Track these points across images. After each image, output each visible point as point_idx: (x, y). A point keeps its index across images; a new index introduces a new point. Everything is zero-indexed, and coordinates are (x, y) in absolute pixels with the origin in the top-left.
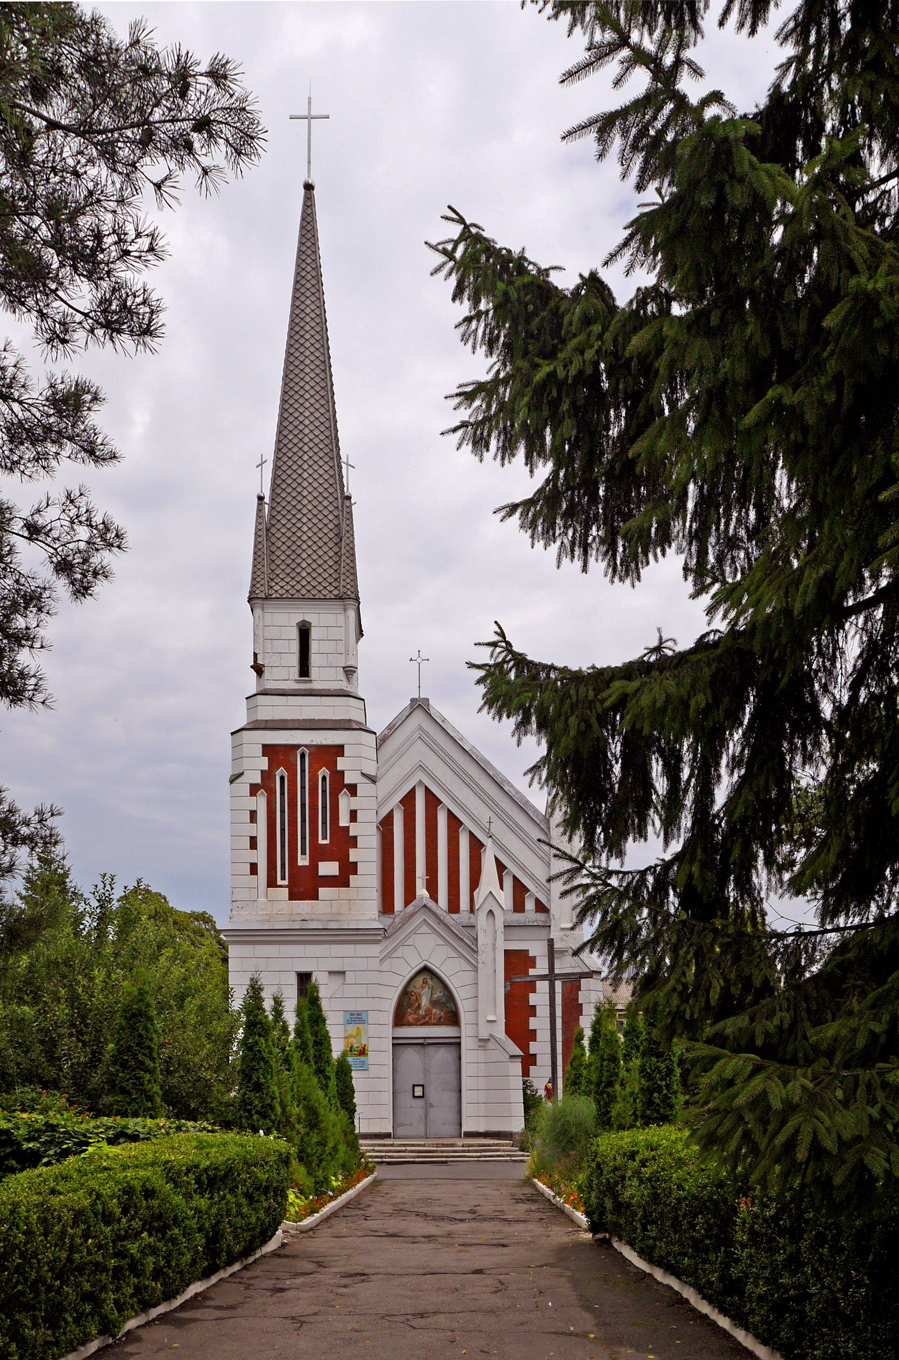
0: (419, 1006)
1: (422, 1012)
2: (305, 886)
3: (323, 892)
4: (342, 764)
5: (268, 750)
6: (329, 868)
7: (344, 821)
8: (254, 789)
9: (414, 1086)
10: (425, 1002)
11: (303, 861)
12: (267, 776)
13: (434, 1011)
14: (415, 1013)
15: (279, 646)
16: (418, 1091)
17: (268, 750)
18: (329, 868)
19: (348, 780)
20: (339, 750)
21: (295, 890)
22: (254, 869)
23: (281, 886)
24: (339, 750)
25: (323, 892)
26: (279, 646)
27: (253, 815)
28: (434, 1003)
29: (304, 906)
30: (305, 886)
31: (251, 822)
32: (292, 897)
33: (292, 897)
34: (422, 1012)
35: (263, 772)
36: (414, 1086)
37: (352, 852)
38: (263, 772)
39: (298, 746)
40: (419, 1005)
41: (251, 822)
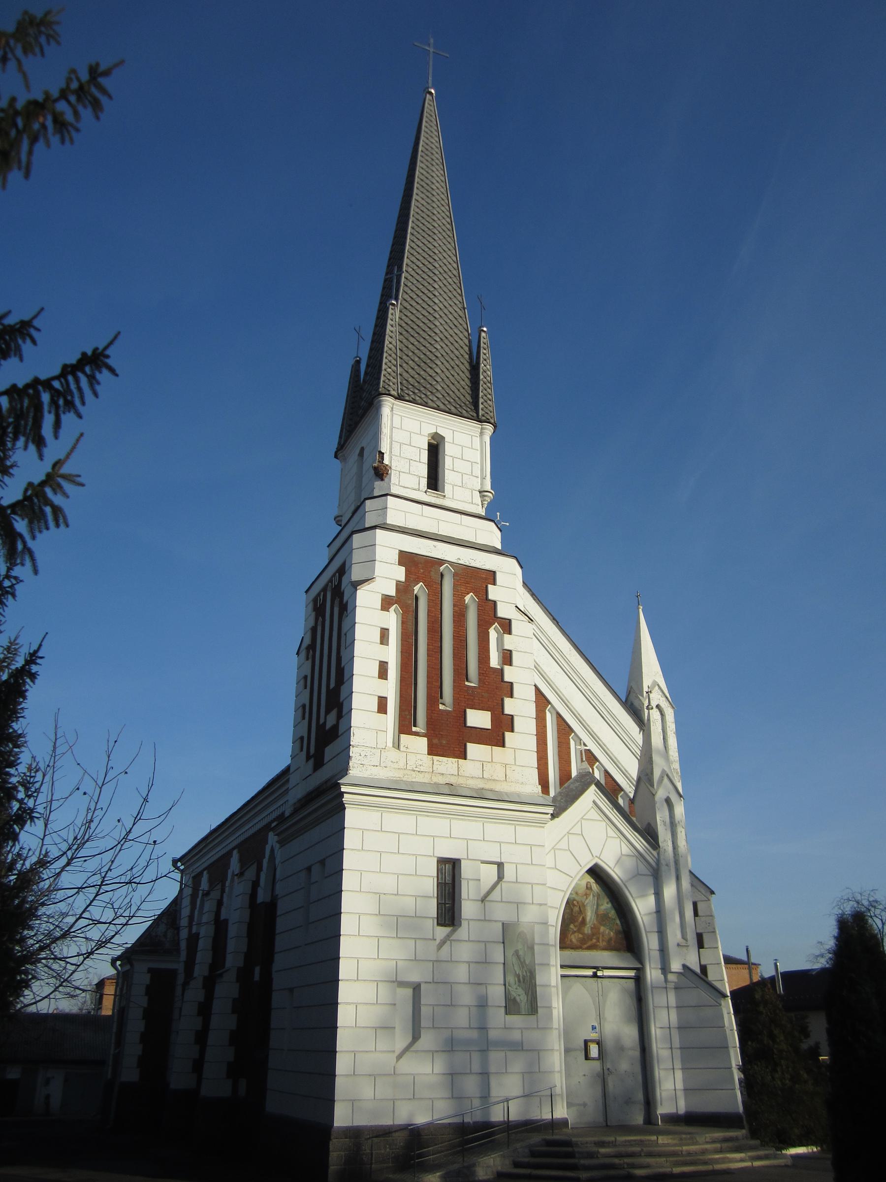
0: (584, 922)
1: (587, 930)
2: (449, 738)
3: (471, 748)
4: (493, 593)
5: (405, 558)
6: (478, 719)
7: (494, 661)
8: (387, 603)
9: (586, 1042)
10: (590, 915)
11: (447, 704)
12: (403, 588)
13: (602, 929)
14: (579, 931)
15: (408, 452)
16: (594, 1051)
17: (406, 559)
18: (478, 719)
19: (502, 612)
20: (491, 577)
21: (435, 741)
22: (382, 706)
23: (417, 734)
24: (491, 577)
25: (471, 748)
26: (408, 452)
27: (384, 635)
28: (602, 918)
29: (447, 765)
30: (449, 738)
31: (382, 643)
32: (433, 750)
33: (433, 750)
34: (587, 930)
35: (398, 583)
36: (586, 1042)
37: (507, 701)
38: (398, 583)
39: (441, 562)
40: (584, 920)
41: (382, 643)
